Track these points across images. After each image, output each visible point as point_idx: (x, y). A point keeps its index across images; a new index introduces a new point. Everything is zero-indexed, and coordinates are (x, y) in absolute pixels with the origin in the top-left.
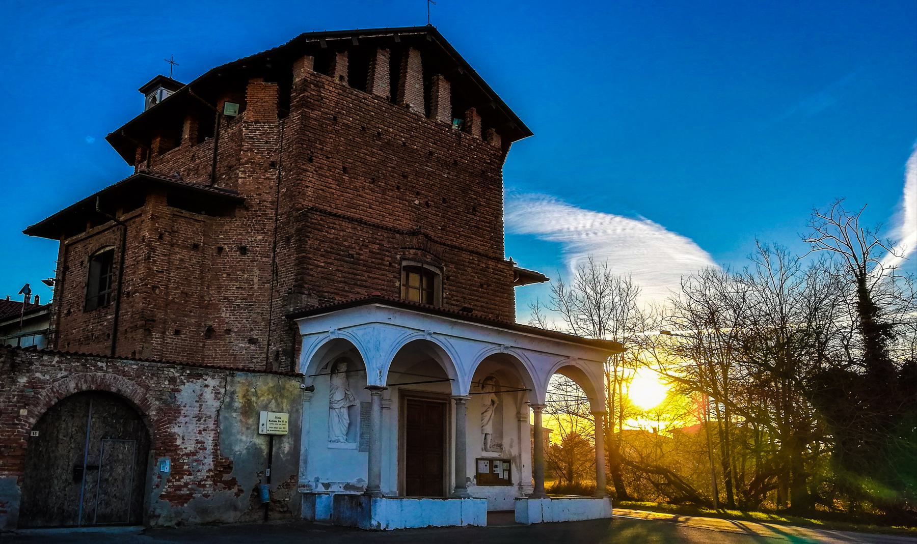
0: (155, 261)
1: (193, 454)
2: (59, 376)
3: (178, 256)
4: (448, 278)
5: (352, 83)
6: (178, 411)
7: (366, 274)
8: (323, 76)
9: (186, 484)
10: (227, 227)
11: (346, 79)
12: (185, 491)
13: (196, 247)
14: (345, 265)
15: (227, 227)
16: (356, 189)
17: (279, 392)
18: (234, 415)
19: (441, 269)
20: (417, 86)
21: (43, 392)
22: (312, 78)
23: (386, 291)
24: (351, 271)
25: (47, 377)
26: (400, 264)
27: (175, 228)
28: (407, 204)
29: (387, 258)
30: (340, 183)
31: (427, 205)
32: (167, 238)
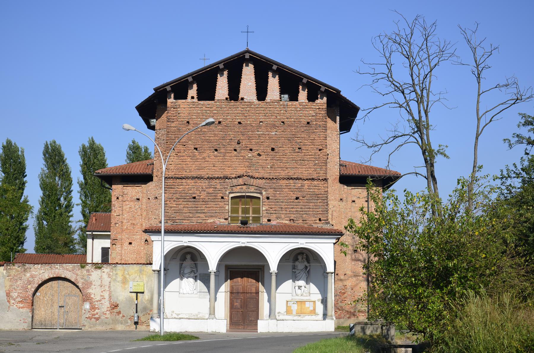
0: (115, 211)
1: (100, 301)
2: (41, 272)
3: (128, 206)
4: (268, 198)
5: (199, 99)
6: (91, 283)
7: (204, 206)
8: (179, 101)
9: (97, 313)
10: (150, 187)
11: (196, 97)
12: (97, 316)
13: (138, 199)
14: (189, 203)
15: (150, 187)
16: (204, 158)
17: (141, 271)
18: (118, 284)
19: (261, 193)
20: (250, 84)
21: (36, 279)
22: (172, 104)
23: (219, 213)
24: (194, 206)
25: (37, 273)
26: (228, 197)
27: (126, 193)
28: (242, 158)
29: (219, 195)
30: (193, 157)
31: (259, 155)
32: (120, 198)
